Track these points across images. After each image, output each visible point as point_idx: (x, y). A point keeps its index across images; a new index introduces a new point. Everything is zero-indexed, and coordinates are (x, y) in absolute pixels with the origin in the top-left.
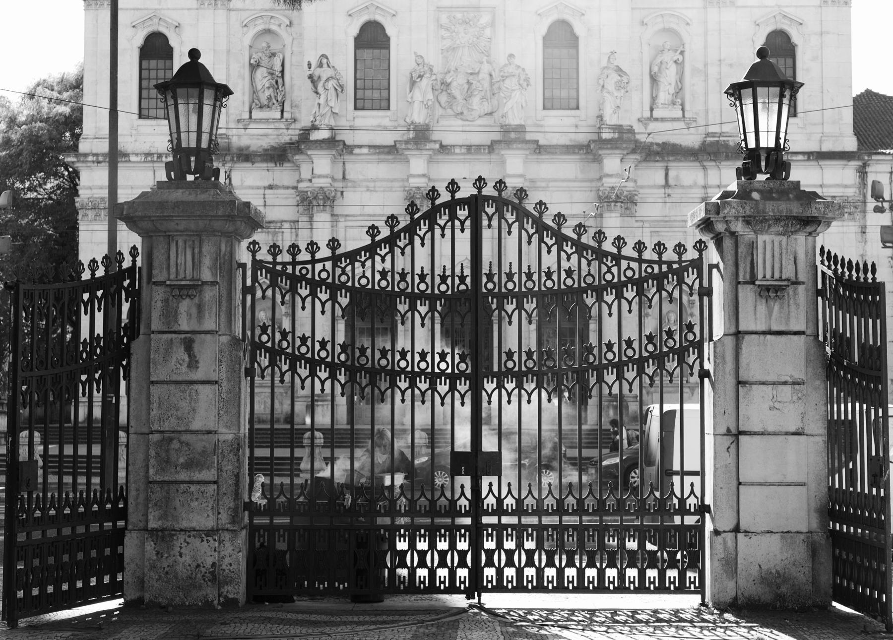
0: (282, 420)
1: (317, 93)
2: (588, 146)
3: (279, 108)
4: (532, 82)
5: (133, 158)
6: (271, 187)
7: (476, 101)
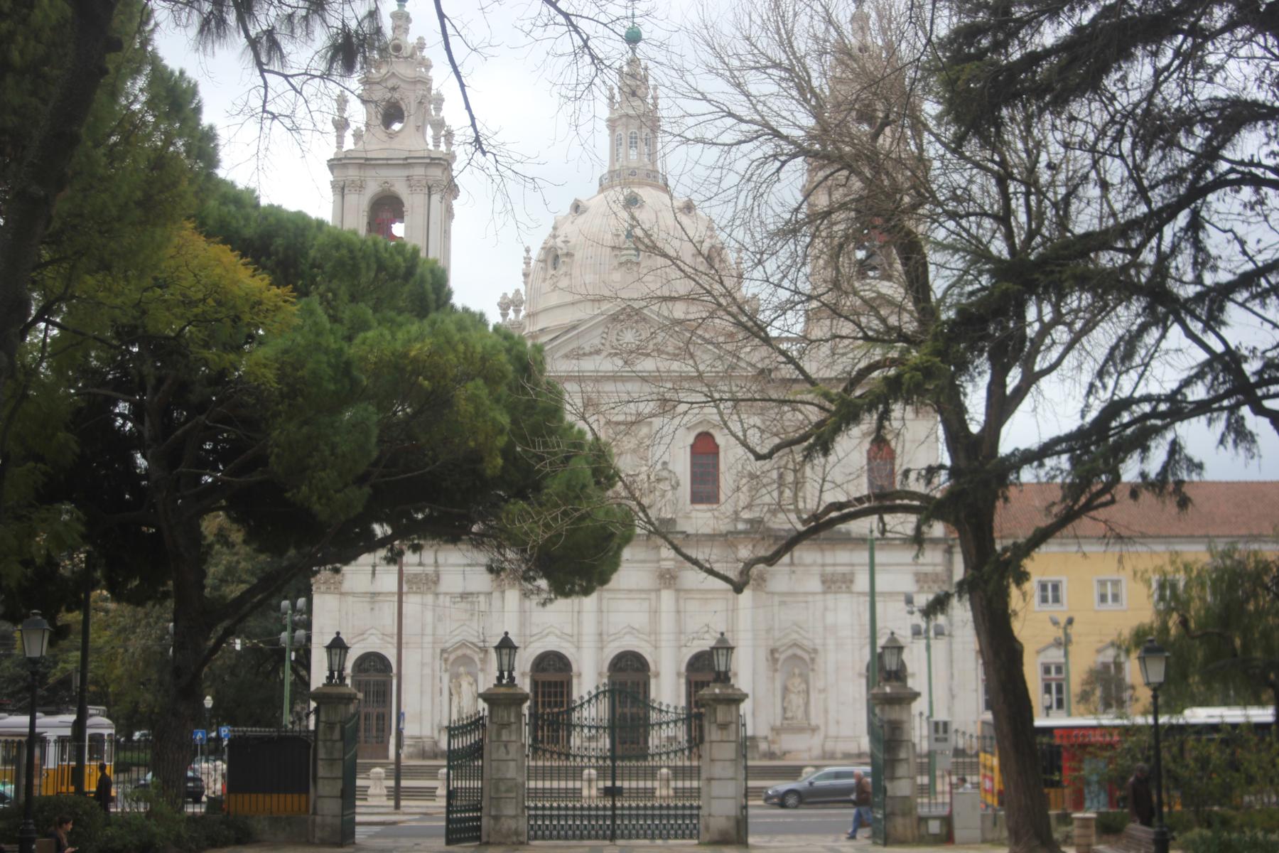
2: (726, 535)
4: (682, 482)
6: (469, 565)
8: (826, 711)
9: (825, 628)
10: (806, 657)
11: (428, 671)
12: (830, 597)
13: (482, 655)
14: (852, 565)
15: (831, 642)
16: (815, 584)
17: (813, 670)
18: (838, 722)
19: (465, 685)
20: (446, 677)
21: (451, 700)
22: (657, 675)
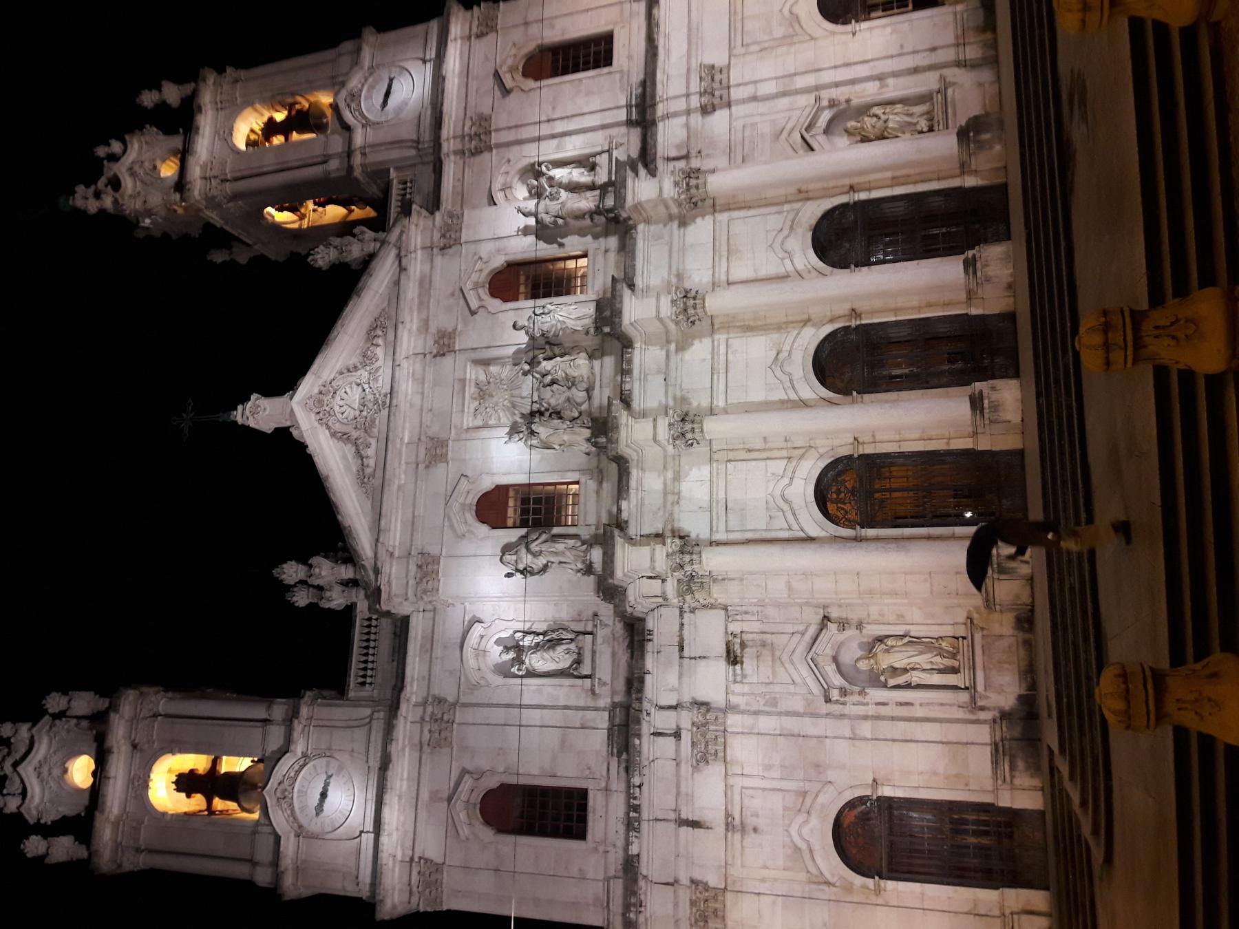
0: (1028, 636)
1: (545, 568)
3: (581, 637)
5: (634, 850)
6: (681, 648)
7: (573, 373)
8: (916, 70)
9: (784, 94)
10: (826, 116)
11: (866, 729)
12: (736, 94)
13: (832, 627)
14: (689, 70)
15: (801, 82)
16: (719, 119)
17: (848, 101)
18: (933, 49)
19: (886, 661)
20: (877, 694)
21: (919, 687)
22: (854, 313)
